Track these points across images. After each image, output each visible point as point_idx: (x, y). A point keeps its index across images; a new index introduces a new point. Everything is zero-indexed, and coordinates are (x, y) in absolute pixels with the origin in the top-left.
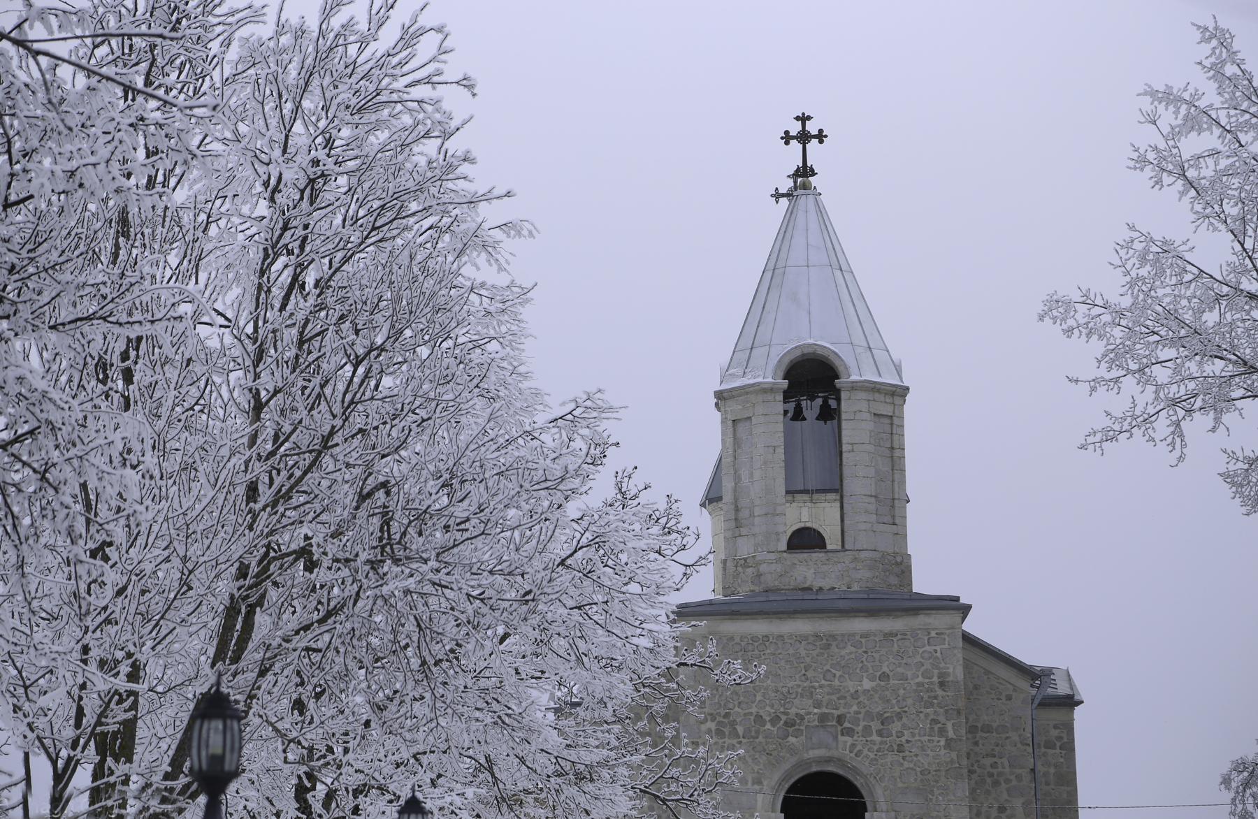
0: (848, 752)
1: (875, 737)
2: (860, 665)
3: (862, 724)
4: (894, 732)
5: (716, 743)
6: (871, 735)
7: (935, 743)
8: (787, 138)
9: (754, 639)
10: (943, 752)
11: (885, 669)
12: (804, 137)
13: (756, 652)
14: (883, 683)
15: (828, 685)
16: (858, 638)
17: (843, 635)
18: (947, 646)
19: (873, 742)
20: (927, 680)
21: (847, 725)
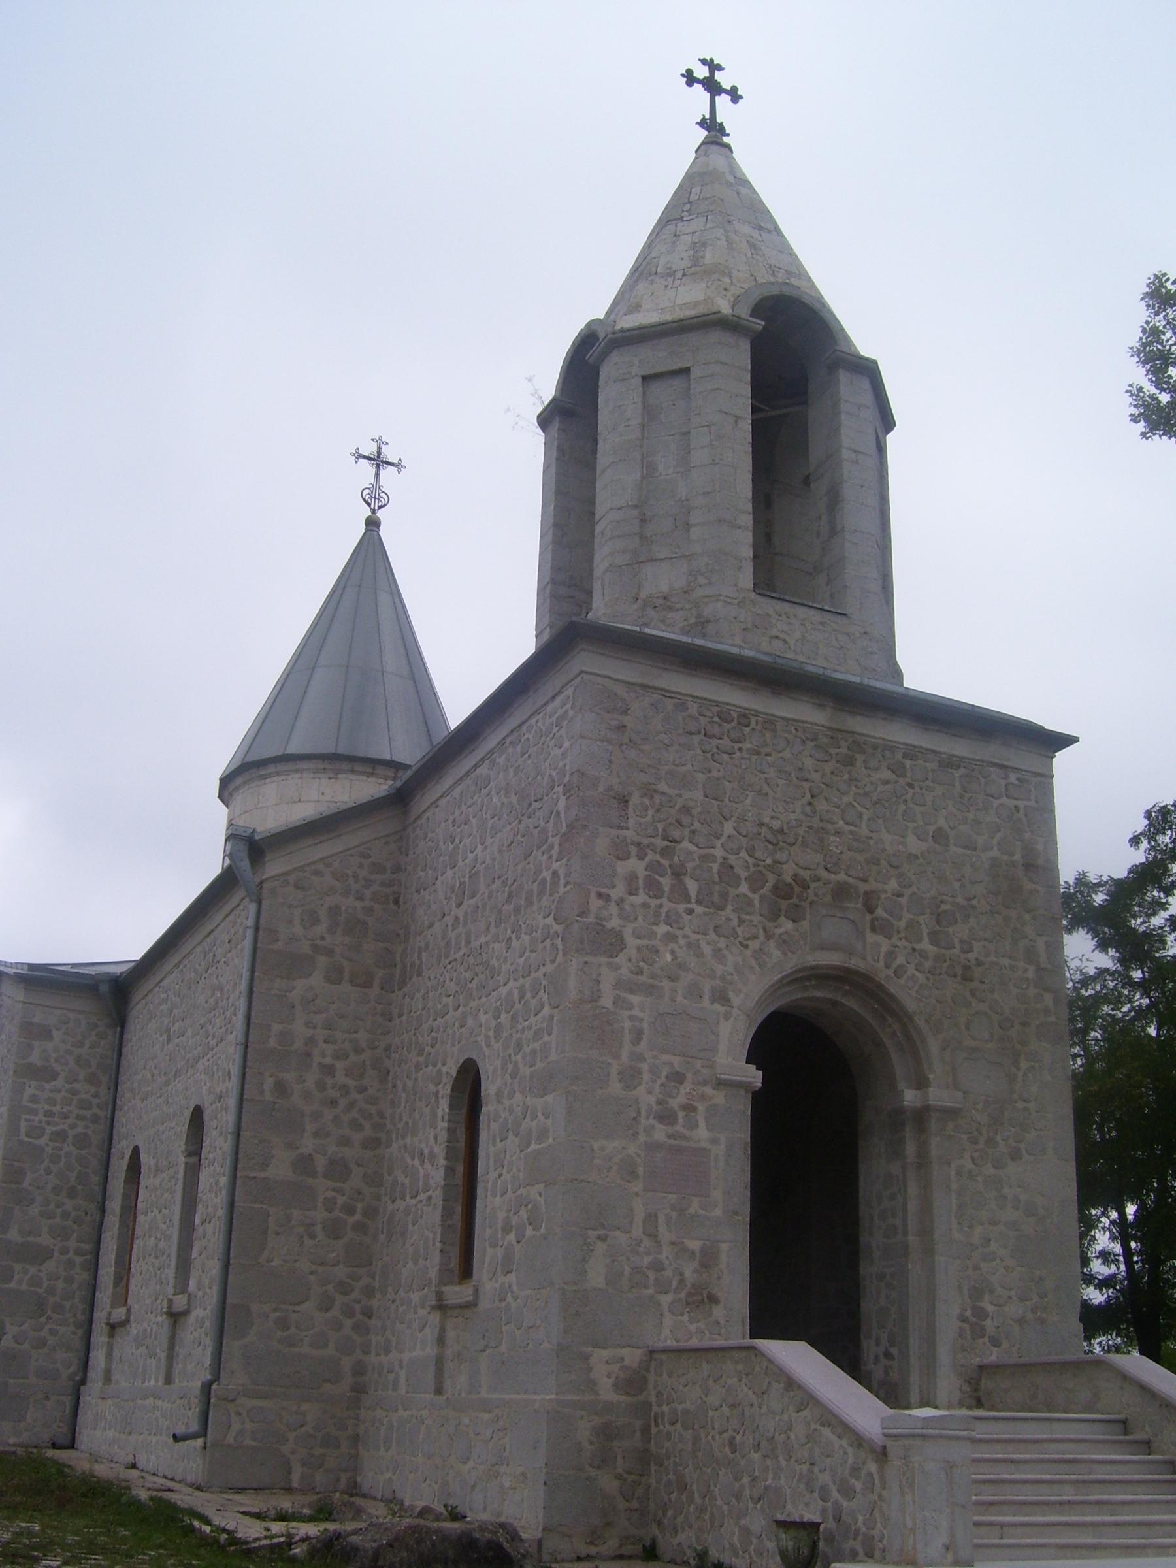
0: (882, 964)
1: (926, 945)
2: (903, 807)
3: (906, 916)
4: (957, 945)
5: (645, 905)
6: (920, 940)
7: (1020, 973)
8: (690, 78)
9: (725, 717)
10: (1032, 991)
11: (942, 822)
12: (712, 87)
13: (725, 743)
14: (938, 848)
15: (851, 832)
16: (899, 756)
17: (875, 747)
18: (1032, 803)
19: (923, 955)
20: (1005, 858)
21: (880, 912)
